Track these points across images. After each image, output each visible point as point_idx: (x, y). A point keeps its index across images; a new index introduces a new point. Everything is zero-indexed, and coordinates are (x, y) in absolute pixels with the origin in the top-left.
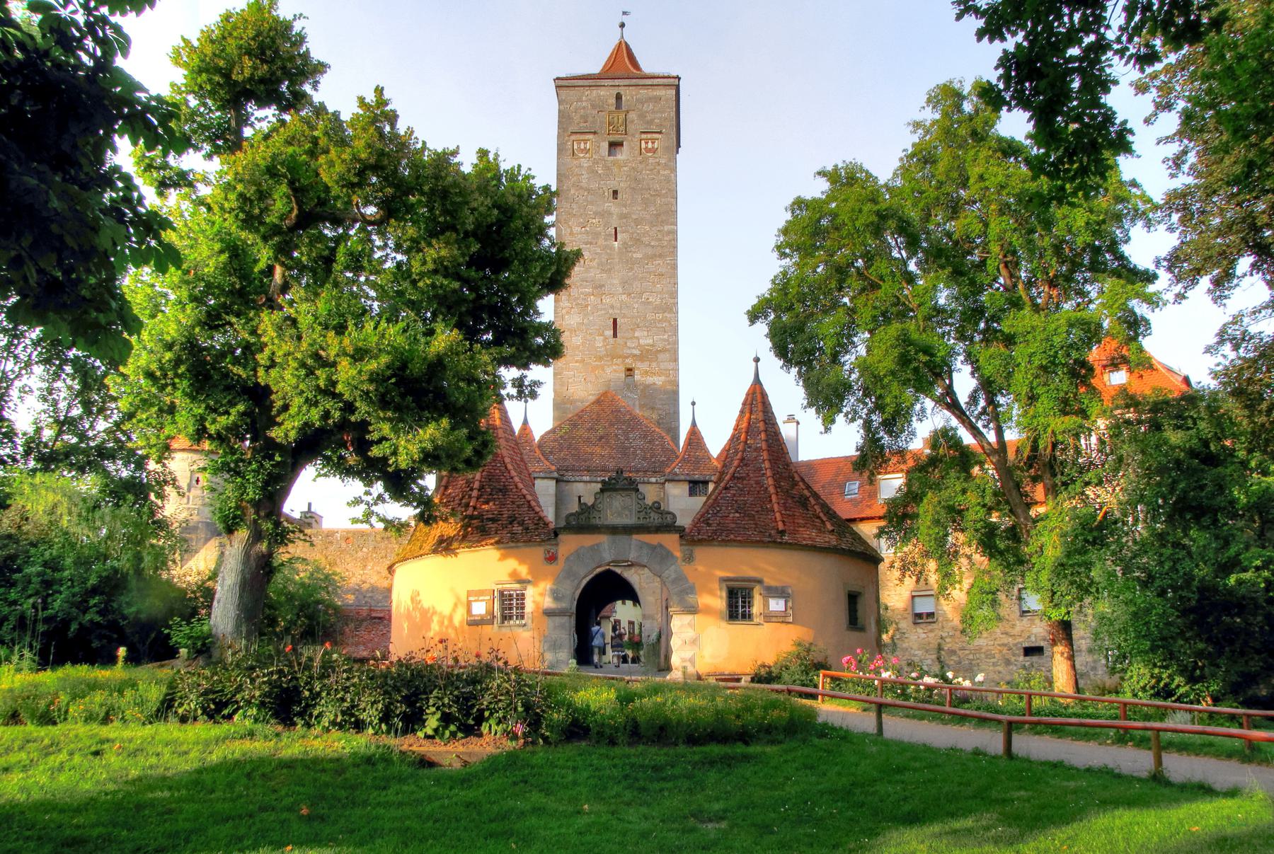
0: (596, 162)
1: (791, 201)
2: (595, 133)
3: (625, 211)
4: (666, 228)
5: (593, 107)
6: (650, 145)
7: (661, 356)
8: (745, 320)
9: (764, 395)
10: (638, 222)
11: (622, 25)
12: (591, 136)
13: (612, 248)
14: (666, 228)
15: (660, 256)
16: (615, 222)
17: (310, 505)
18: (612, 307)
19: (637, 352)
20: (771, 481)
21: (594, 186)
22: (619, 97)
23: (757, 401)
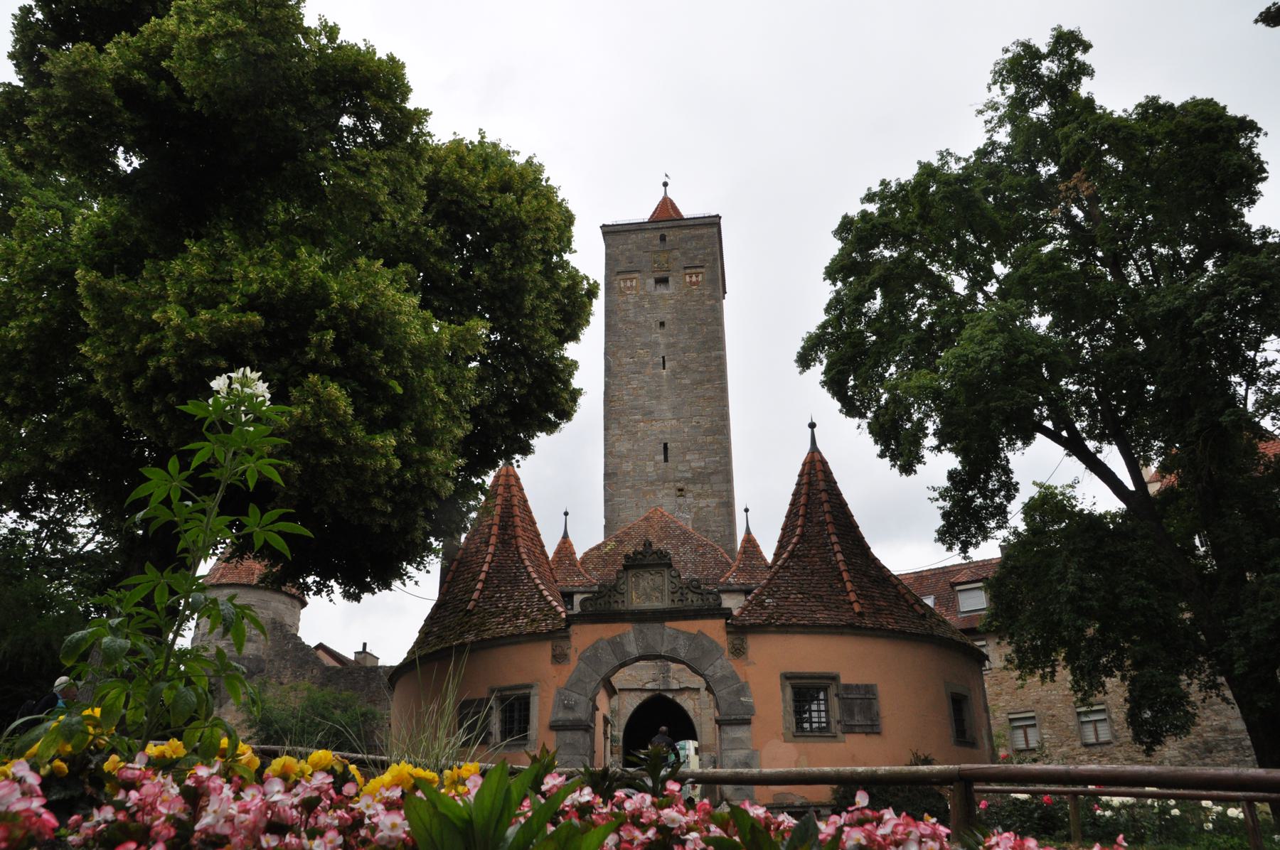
0: (642, 298)
1: (835, 224)
2: (639, 271)
3: (672, 340)
4: (714, 354)
5: (639, 248)
6: (694, 279)
7: (713, 478)
8: (795, 368)
9: (824, 463)
10: (685, 350)
11: (665, 184)
12: (636, 275)
13: (660, 376)
14: (714, 354)
15: (708, 381)
16: (662, 351)
17: (365, 645)
18: (662, 432)
19: (689, 475)
20: (840, 557)
21: (641, 319)
22: (663, 238)
23: (816, 483)
